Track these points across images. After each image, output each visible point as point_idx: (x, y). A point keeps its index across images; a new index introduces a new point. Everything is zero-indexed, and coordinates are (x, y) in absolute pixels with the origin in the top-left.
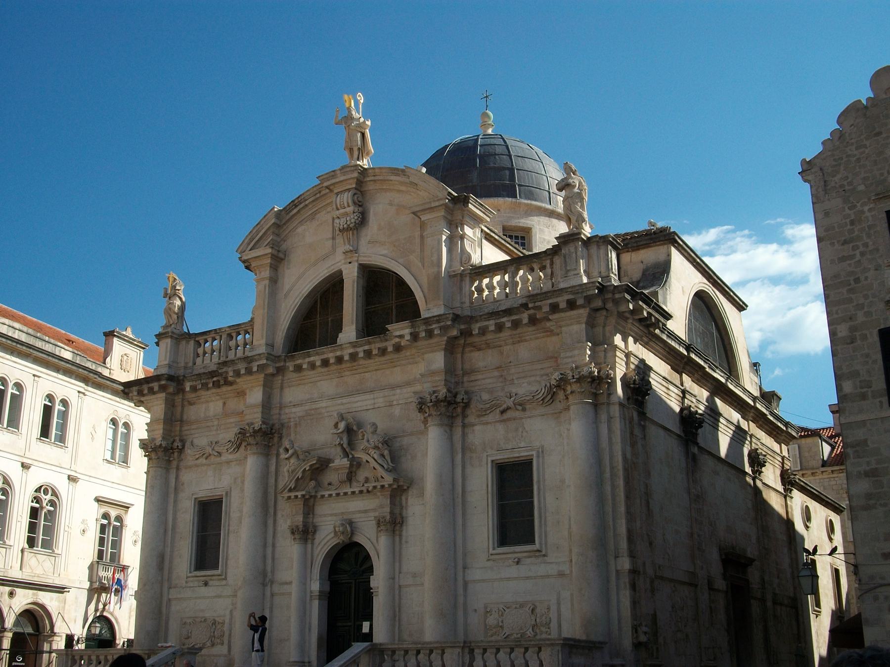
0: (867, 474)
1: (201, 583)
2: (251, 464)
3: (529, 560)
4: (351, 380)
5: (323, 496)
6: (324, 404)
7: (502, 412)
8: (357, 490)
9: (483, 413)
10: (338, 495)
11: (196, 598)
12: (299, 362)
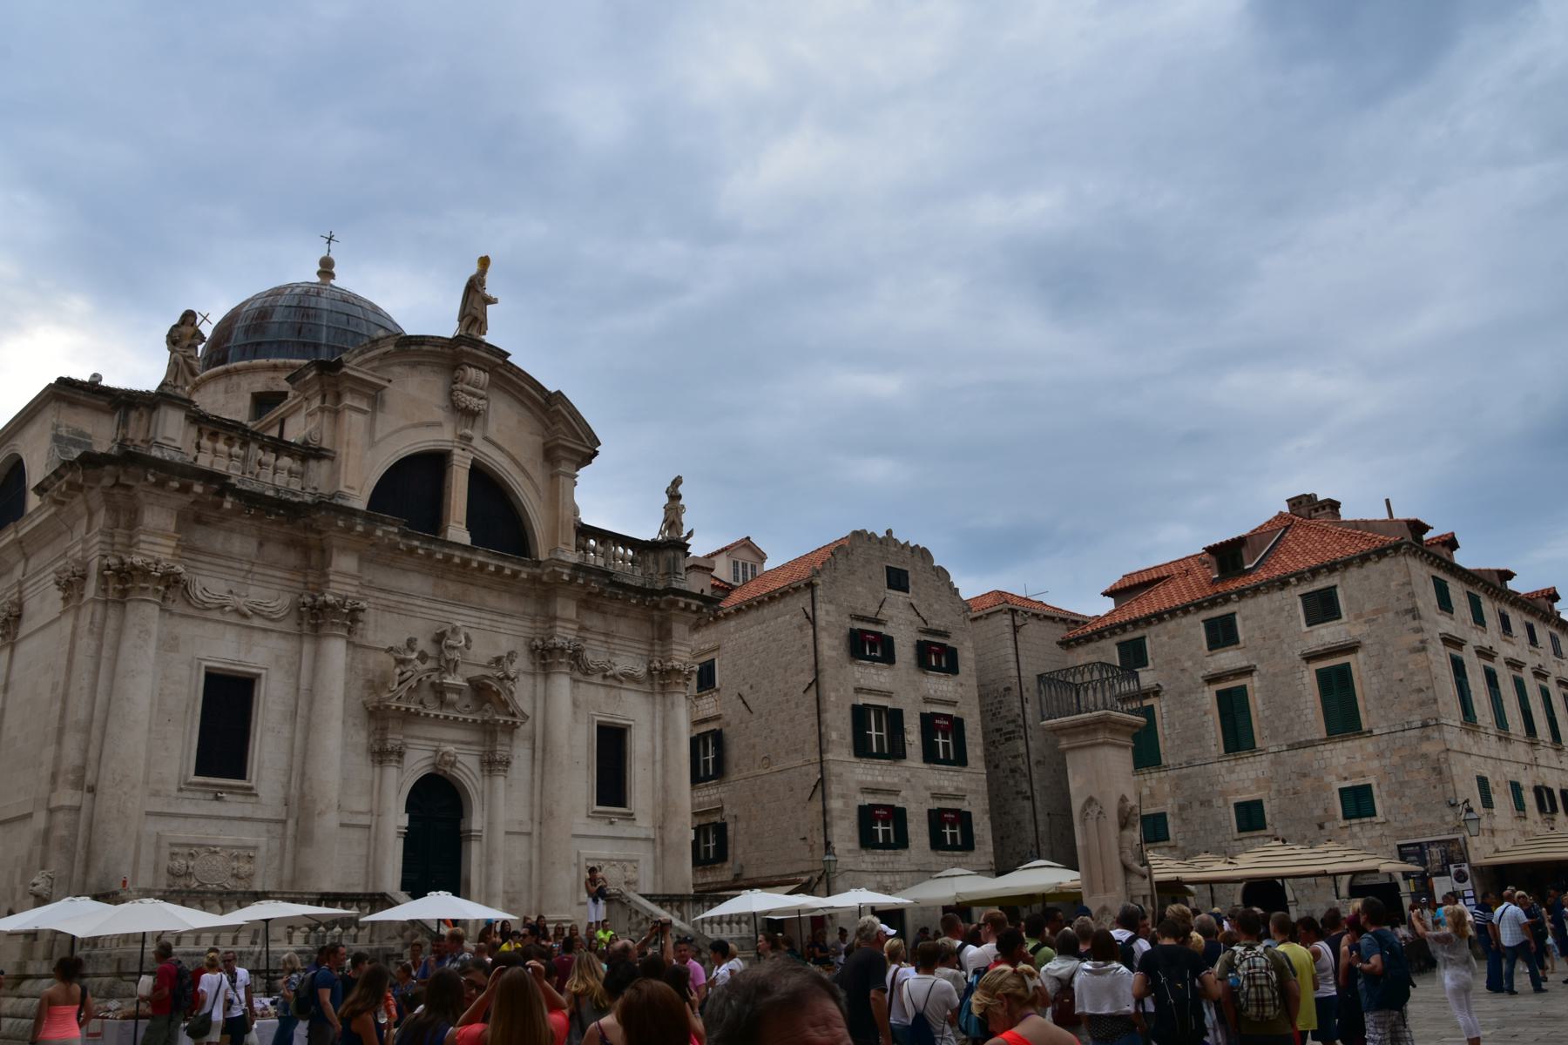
0: (843, 796)
1: (211, 796)
4: (453, 588)
5: (427, 715)
6: (419, 602)
7: (605, 677)
8: (461, 717)
10: (446, 718)
11: (202, 817)
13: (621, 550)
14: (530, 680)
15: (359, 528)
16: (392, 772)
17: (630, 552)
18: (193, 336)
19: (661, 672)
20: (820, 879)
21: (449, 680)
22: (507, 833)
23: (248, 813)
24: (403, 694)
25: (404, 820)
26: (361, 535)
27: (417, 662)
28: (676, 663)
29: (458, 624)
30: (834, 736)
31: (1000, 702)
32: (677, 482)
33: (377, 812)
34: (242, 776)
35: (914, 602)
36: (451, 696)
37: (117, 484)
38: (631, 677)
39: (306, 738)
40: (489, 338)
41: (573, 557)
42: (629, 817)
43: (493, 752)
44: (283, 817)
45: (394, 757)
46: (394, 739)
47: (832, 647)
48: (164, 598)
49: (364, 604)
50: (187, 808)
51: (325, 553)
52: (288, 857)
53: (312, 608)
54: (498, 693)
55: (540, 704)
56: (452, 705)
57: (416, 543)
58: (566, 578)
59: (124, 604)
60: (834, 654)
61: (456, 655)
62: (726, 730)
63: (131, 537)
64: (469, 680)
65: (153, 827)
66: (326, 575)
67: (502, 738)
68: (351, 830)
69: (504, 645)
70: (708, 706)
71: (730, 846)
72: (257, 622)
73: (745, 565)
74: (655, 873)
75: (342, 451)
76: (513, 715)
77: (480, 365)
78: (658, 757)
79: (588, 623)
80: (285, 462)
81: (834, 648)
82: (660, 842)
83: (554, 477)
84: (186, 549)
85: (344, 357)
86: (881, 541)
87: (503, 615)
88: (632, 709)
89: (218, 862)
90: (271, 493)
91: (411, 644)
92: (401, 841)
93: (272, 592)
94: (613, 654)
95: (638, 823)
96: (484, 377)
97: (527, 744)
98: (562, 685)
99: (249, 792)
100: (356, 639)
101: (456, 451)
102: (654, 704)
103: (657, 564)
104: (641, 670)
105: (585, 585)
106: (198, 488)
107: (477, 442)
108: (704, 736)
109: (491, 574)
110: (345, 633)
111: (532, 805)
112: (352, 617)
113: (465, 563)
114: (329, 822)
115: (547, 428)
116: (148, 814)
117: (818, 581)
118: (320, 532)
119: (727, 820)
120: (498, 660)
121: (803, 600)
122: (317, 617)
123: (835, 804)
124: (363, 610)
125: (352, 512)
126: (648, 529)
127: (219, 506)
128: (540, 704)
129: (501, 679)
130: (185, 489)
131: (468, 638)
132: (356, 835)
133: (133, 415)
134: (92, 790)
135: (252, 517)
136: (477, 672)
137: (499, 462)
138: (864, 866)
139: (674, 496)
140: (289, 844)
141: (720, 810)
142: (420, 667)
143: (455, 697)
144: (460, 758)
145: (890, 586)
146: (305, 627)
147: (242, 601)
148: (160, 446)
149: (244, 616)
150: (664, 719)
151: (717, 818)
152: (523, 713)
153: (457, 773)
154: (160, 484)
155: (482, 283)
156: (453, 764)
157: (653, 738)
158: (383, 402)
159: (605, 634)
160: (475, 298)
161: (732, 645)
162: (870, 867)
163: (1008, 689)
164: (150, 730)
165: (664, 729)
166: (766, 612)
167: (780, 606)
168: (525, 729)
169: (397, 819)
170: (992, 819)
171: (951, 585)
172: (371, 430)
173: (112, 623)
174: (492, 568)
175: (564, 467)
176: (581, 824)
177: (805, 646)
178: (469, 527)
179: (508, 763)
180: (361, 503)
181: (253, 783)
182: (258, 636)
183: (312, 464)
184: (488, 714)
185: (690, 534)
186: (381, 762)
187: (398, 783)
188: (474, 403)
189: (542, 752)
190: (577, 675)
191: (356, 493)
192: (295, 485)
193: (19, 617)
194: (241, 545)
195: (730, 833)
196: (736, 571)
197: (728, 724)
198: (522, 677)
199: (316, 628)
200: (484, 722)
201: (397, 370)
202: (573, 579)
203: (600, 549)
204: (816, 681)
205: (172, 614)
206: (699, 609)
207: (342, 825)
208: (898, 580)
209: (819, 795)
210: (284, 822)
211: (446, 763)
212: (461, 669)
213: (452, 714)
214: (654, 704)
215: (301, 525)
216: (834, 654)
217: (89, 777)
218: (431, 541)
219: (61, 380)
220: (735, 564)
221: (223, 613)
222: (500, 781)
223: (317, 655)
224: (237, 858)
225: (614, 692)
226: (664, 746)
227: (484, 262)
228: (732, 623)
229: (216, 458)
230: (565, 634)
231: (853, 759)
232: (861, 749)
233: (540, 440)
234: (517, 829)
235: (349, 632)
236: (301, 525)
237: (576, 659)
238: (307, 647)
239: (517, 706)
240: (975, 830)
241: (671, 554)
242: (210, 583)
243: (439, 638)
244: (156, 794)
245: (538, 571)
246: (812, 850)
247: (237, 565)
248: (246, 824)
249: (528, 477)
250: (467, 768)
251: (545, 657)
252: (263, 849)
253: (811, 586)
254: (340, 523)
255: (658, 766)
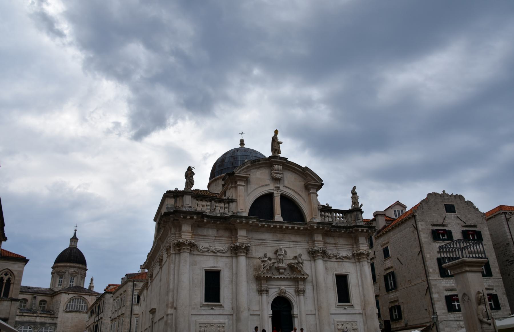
0: (438, 293)
1: (210, 308)
2: (242, 260)
3: (349, 308)
4: (279, 236)
9: (330, 257)
10: (281, 278)
12: (264, 223)
13: (338, 214)
14: (309, 262)
15: (244, 222)
16: (265, 297)
17: (341, 215)
18: (191, 173)
19: (357, 254)
20: (433, 324)
21: (280, 265)
22: (307, 314)
23: (221, 313)
24: (265, 271)
25: (271, 312)
26: (245, 223)
27: (268, 261)
28: (361, 251)
29: (281, 247)
30: (431, 270)
31: (506, 249)
32: (354, 188)
33: (261, 310)
34: (218, 301)
35: (459, 216)
36: (282, 271)
37: (174, 220)
38: (346, 257)
39: (236, 288)
40: (281, 155)
41: (318, 220)
42: (352, 306)
43: (298, 288)
44: (232, 313)
45: (265, 292)
46: (264, 286)
47: (425, 237)
48: (191, 250)
49: (249, 245)
50: (203, 312)
51: (236, 231)
52: (235, 326)
53: (234, 248)
54: (297, 268)
55: (313, 270)
56: (282, 273)
57: (264, 223)
58: (315, 227)
59: (180, 253)
60: (426, 240)
61: (282, 257)
62: (395, 272)
63: (180, 234)
64: (288, 265)
65: (194, 318)
66: (237, 237)
67: (301, 283)
68: (254, 316)
69: (299, 251)
70: (388, 263)
71: (402, 313)
72: (219, 254)
73: (398, 211)
74: (364, 325)
75: (238, 199)
76: (303, 275)
77: (279, 163)
78: (360, 284)
79: (328, 241)
80: (222, 205)
81: (426, 238)
82: (364, 313)
83: (309, 194)
84: (195, 235)
85: (235, 170)
86: (440, 195)
87: (297, 242)
88: (349, 268)
89: (213, 328)
90: (219, 215)
91: (265, 255)
92: (270, 319)
93: (222, 245)
94: (339, 250)
95: (355, 308)
96: (280, 167)
97: (311, 284)
98: (320, 263)
99: (221, 306)
100: (249, 256)
101: (275, 192)
102: (356, 266)
103: (351, 217)
104: (350, 254)
105: (323, 228)
106: (195, 217)
107: (282, 188)
108: (389, 274)
109: (291, 229)
110: (245, 255)
111: (315, 305)
112: (247, 249)
113: (281, 227)
114: (245, 314)
115: (305, 179)
116: (192, 315)
117: (416, 214)
118: (234, 224)
119: (400, 304)
120: (296, 257)
121: (412, 222)
122: (236, 251)
123: (435, 296)
124: (249, 247)
125: (241, 217)
126: (348, 206)
127: (203, 221)
128: (313, 270)
129: (297, 264)
130: (192, 218)
131: (285, 251)
132: (255, 318)
133: (178, 199)
134: (175, 309)
135: (213, 223)
136: (289, 262)
137: (290, 193)
138: (450, 319)
139: (354, 193)
140: (234, 322)
141: (397, 301)
142: (270, 262)
143: (283, 271)
144: (287, 290)
145: (447, 212)
146: (233, 255)
147: (213, 248)
148: (185, 207)
149: (215, 253)
150: (361, 270)
151: (397, 304)
152: (306, 274)
153: (287, 296)
154: (185, 218)
155: (277, 138)
156: (285, 293)
157: (357, 278)
158: (250, 182)
159: (335, 244)
160: (275, 144)
161: (395, 240)
162: (453, 319)
163: (508, 244)
164: (190, 289)
165: (361, 274)
166: (401, 228)
167: (405, 225)
168: (309, 278)
169: (268, 312)
170: (507, 296)
171: (474, 207)
172: (247, 190)
173: (177, 259)
174: (290, 228)
175: (312, 191)
176: (334, 309)
177: (415, 238)
178: (282, 215)
179: (304, 291)
180: (246, 214)
181: (222, 304)
182: (219, 258)
183: (231, 204)
184: (296, 275)
185: (361, 205)
186: (261, 294)
187: (267, 301)
188: (278, 176)
189: (316, 287)
190: (326, 259)
191: (244, 211)
192: (226, 211)
193: (162, 260)
194: (212, 232)
195: (402, 309)
196: (395, 214)
197: (396, 269)
198: (305, 262)
199: (236, 254)
200: (294, 278)
201: (253, 171)
202: (318, 228)
203: (329, 215)
204: (421, 250)
205: (194, 255)
206: (367, 231)
207: (251, 315)
208: (450, 209)
209: (428, 293)
210: (232, 315)
211: (283, 293)
212: (285, 261)
213: (283, 276)
214: (356, 266)
215: (228, 224)
216: (426, 240)
217: (175, 305)
218: (269, 222)
219: (167, 192)
220: (395, 211)
221: (209, 253)
222: (302, 297)
223: (237, 262)
224: (219, 327)
225: (340, 263)
226: (362, 280)
227: (276, 132)
228: (392, 233)
229: (203, 207)
230: (319, 246)
231: (441, 278)
232: (443, 273)
233: (303, 183)
234: (310, 313)
235: (246, 254)
236: (228, 224)
237: (324, 254)
238: (234, 260)
239: (304, 272)
240: (500, 301)
241: (355, 213)
242: (203, 245)
243: (276, 252)
244: (194, 309)
245: (306, 226)
246: (429, 314)
247: (211, 238)
248: (221, 316)
249: (300, 196)
250: (290, 293)
251: (313, 254)
252: (227, 324)
253: (414, 216)
254: (238, 221)
255: (361, 288)
